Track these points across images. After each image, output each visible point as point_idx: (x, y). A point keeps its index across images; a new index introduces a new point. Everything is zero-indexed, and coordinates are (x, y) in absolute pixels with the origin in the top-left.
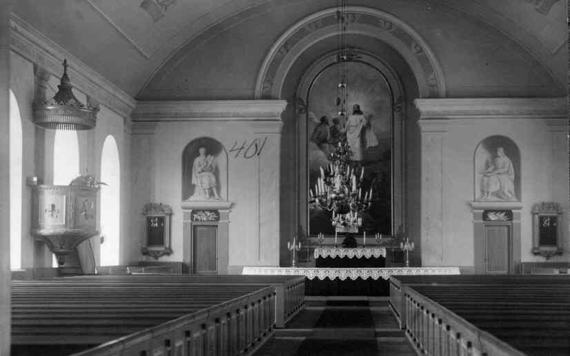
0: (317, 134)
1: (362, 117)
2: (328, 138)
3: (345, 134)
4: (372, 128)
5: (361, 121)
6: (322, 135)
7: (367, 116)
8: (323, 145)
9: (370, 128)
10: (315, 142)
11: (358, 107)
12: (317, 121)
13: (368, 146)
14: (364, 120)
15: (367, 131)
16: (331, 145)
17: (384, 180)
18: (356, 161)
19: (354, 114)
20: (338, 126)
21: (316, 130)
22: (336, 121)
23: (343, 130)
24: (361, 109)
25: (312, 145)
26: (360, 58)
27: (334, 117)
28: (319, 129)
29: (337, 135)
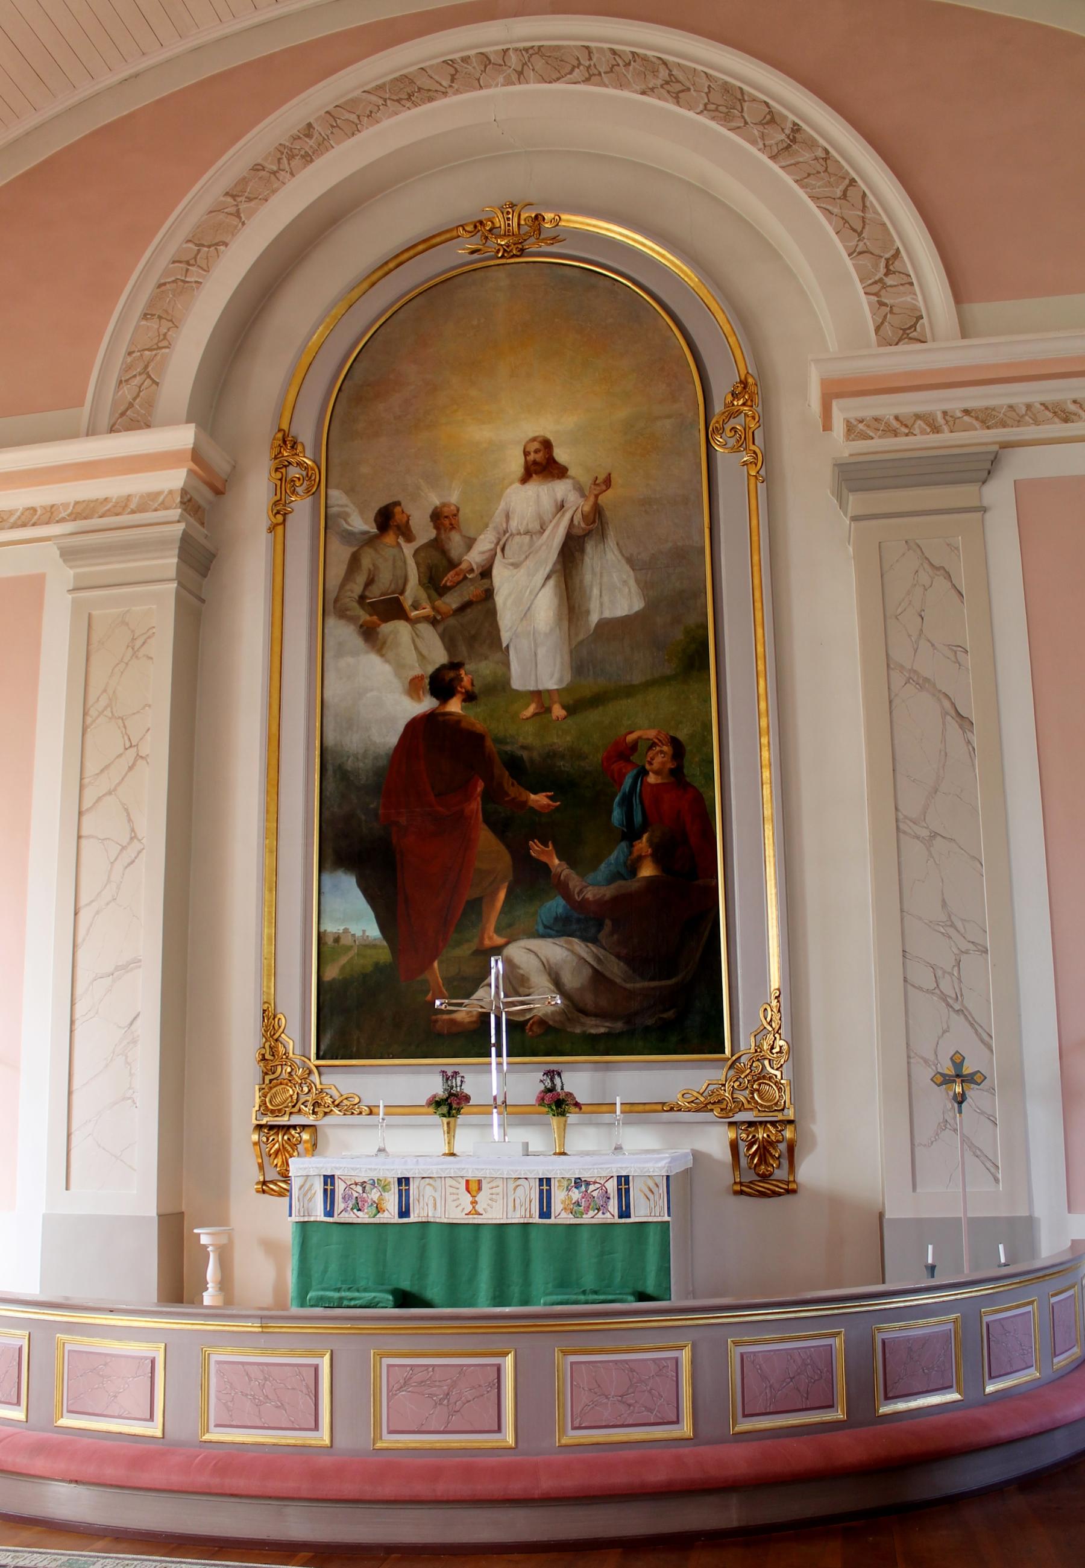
0: (361, 579)
1: (561, 489)
2: (407, 601)
3: (486, 573)
4: (611, 533)
5: (561, 507)
6: (385, 581)
7: (586, 480)
8: (386, 628)
9: (603, 536)
10: (351, 619)
11: (547, 445)
12: (361, 523)
13: (594, 618)
14: (573, 499)
15: (589, 547)
16: (425, 629)
17: (677, 773)
18: (537, 695)
19: (526, 478)
20: (455, 542)
21: (354, 562)
22: (437, 517)
23: (475, 557)
24: (561, 455)
25: (344, 633)
26: (555, 239)
27: (434, 500)
28: (366, 562)
29: (449, 578)
